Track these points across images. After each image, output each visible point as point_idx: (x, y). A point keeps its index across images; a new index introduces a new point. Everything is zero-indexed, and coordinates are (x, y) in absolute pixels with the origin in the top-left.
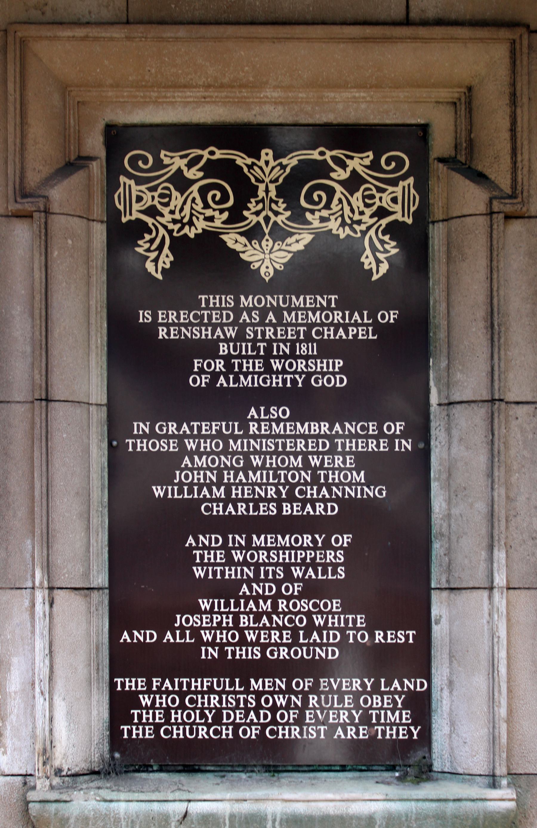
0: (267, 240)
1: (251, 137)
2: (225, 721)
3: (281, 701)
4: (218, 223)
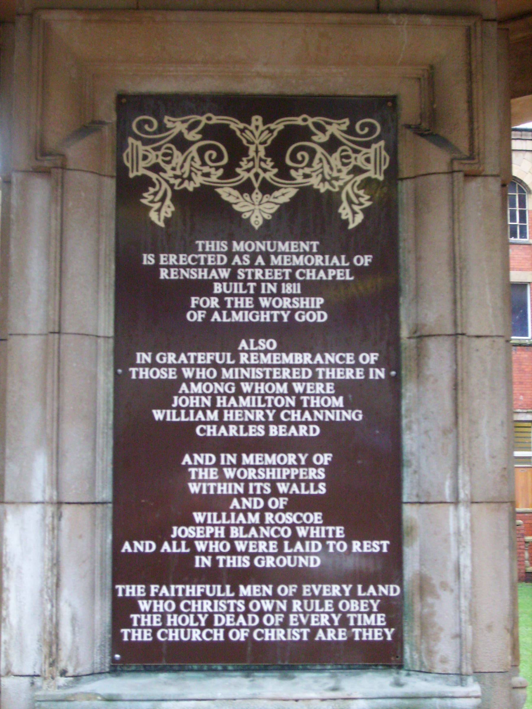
0: (257, 194)
2: (216, 624)
3: (268, 605)
4: (214, 179)
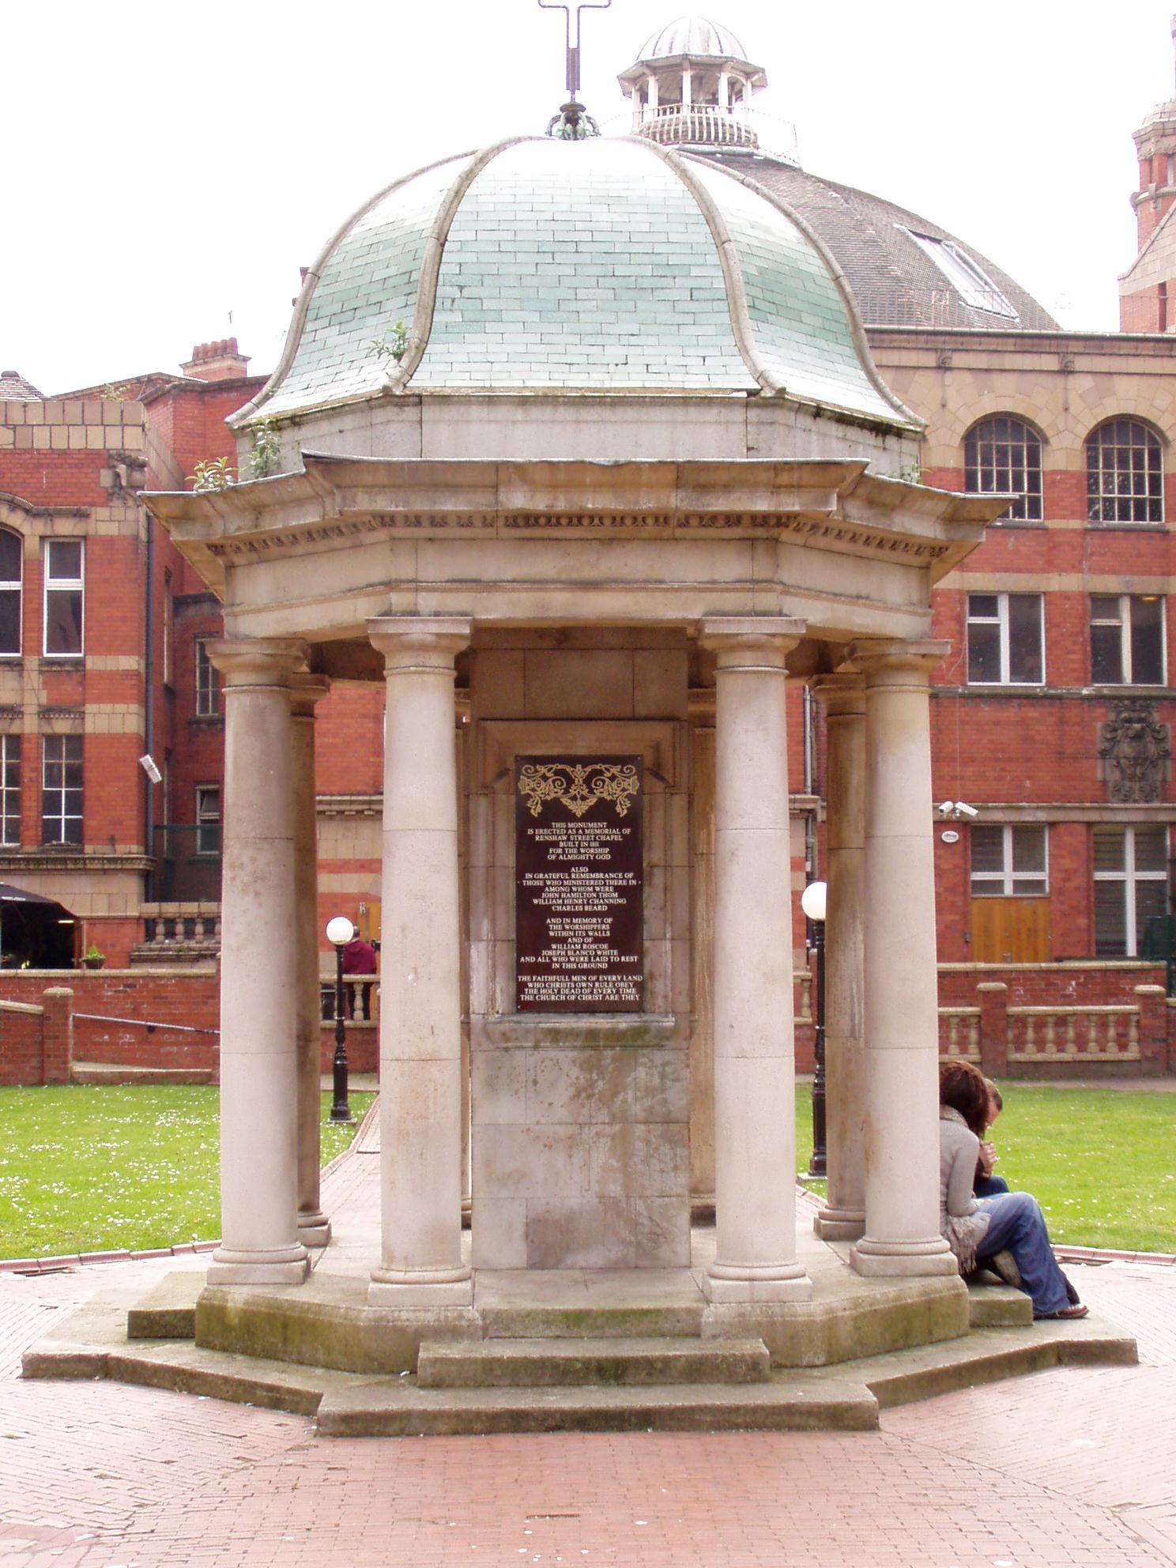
1: (573, 761)
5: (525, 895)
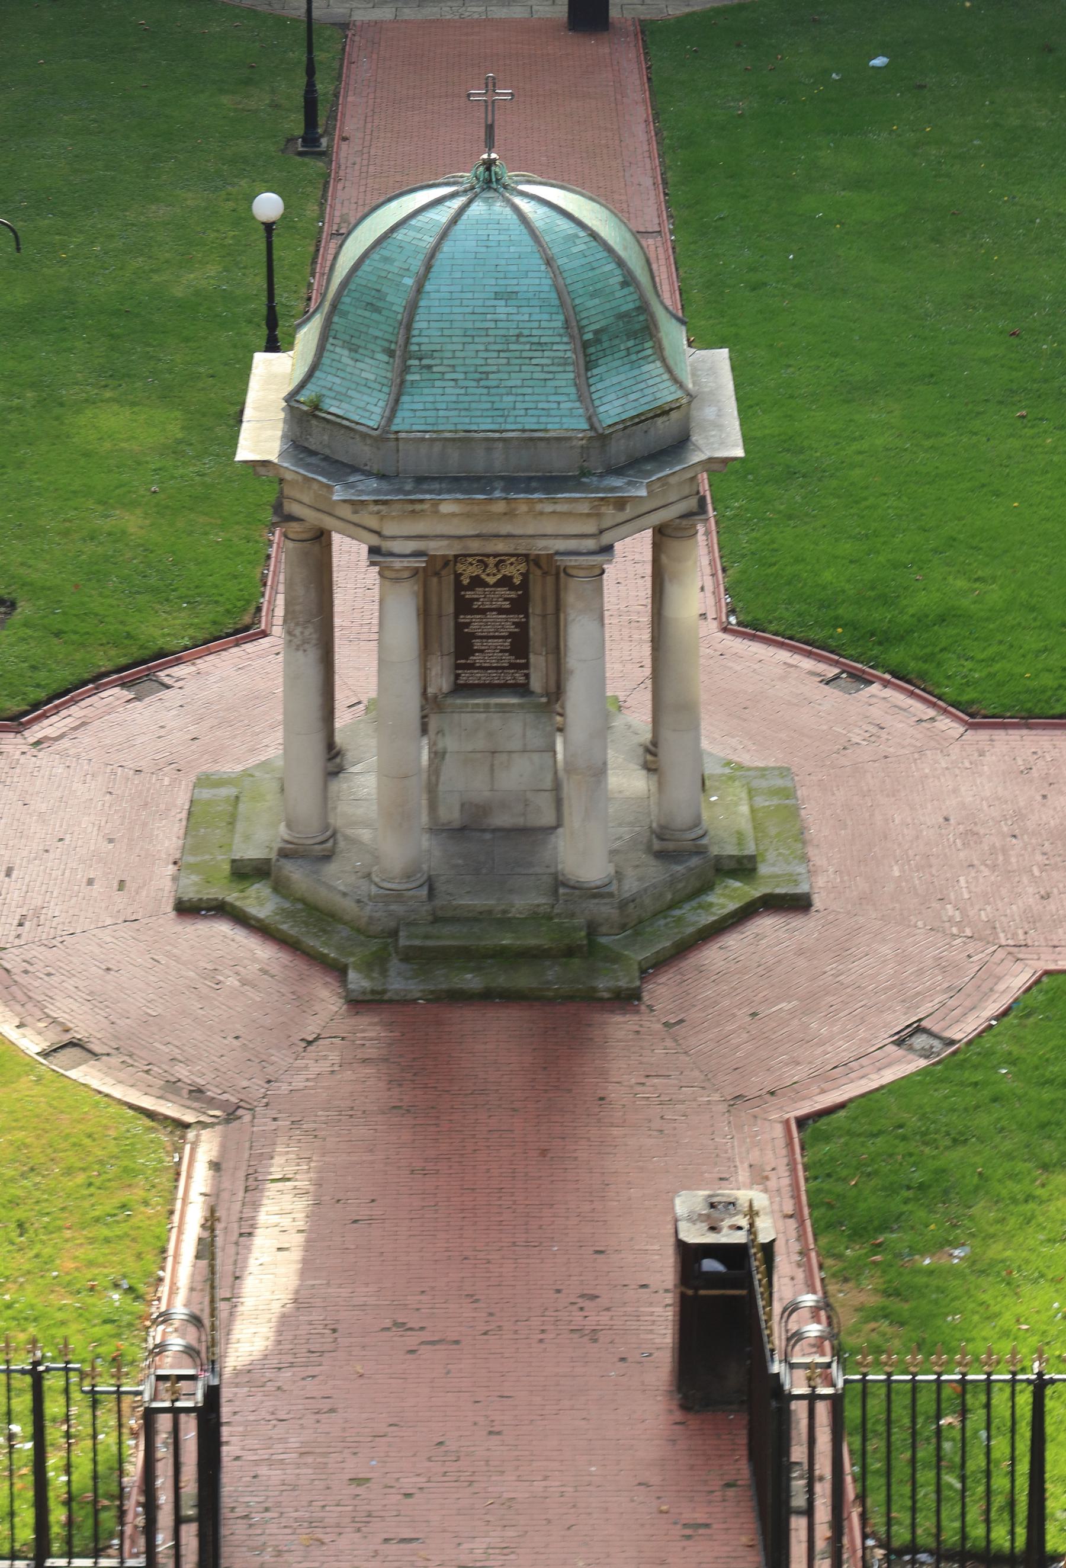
1: (488, 556)
5: (459, 627)
